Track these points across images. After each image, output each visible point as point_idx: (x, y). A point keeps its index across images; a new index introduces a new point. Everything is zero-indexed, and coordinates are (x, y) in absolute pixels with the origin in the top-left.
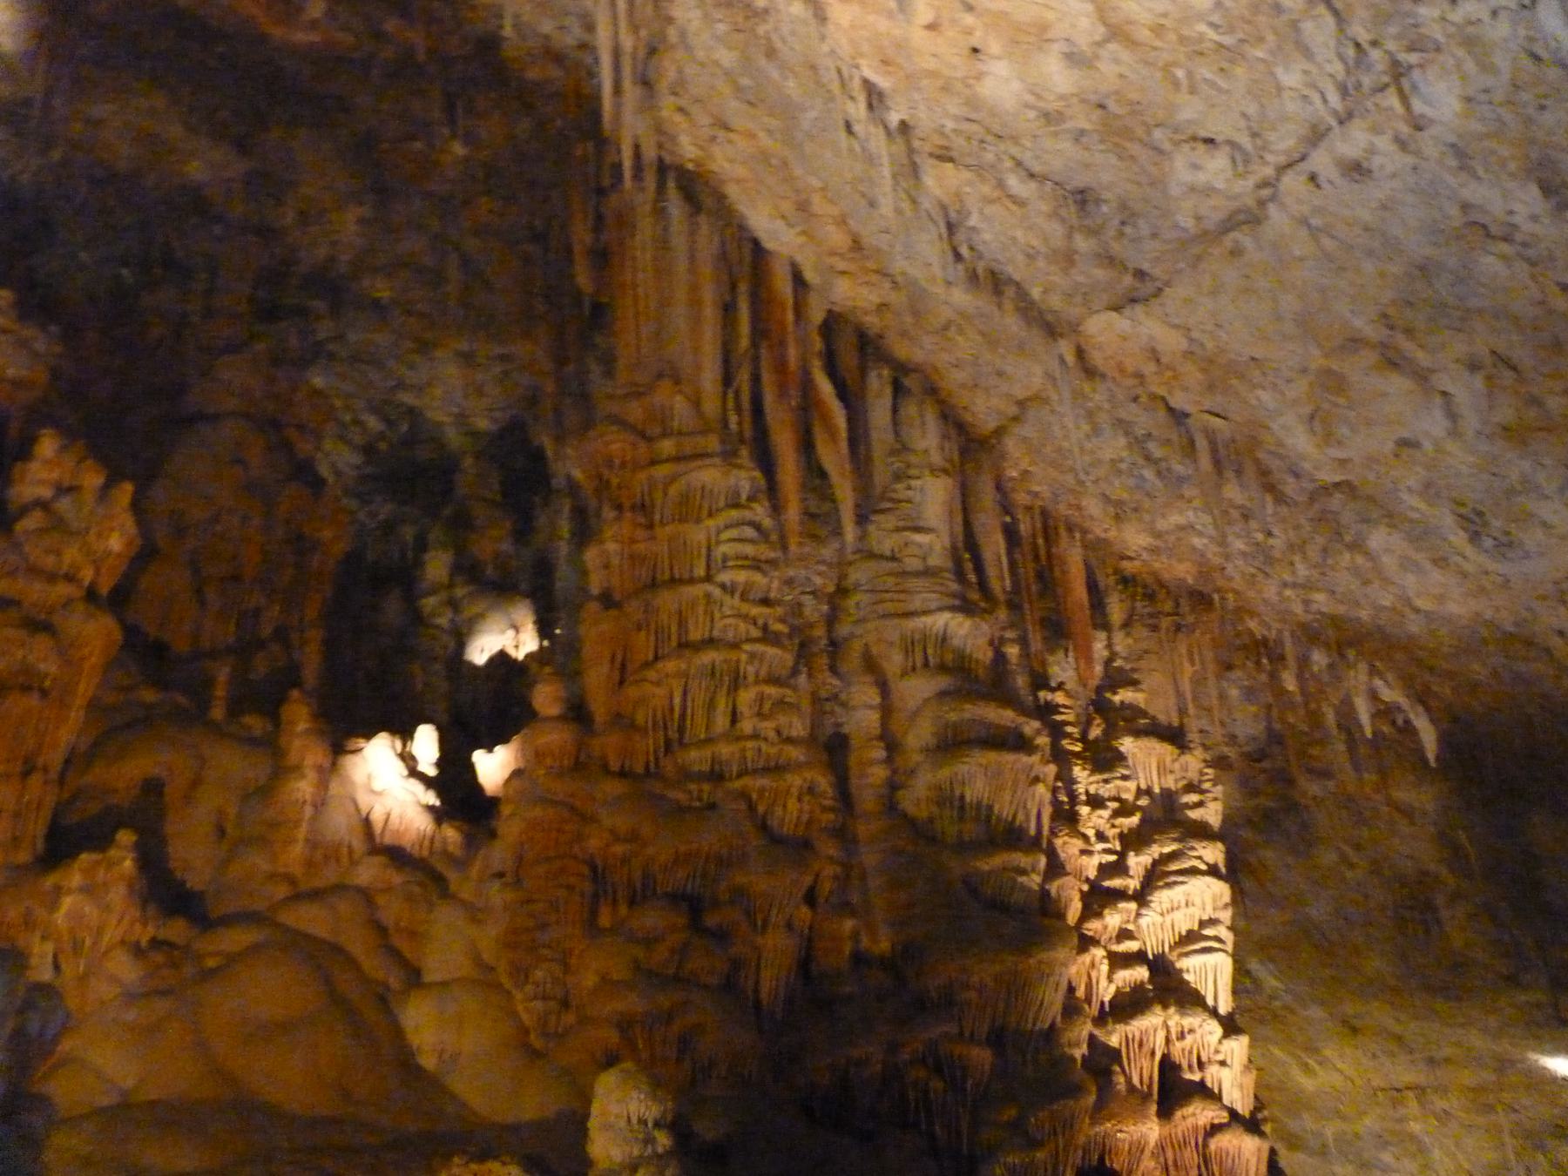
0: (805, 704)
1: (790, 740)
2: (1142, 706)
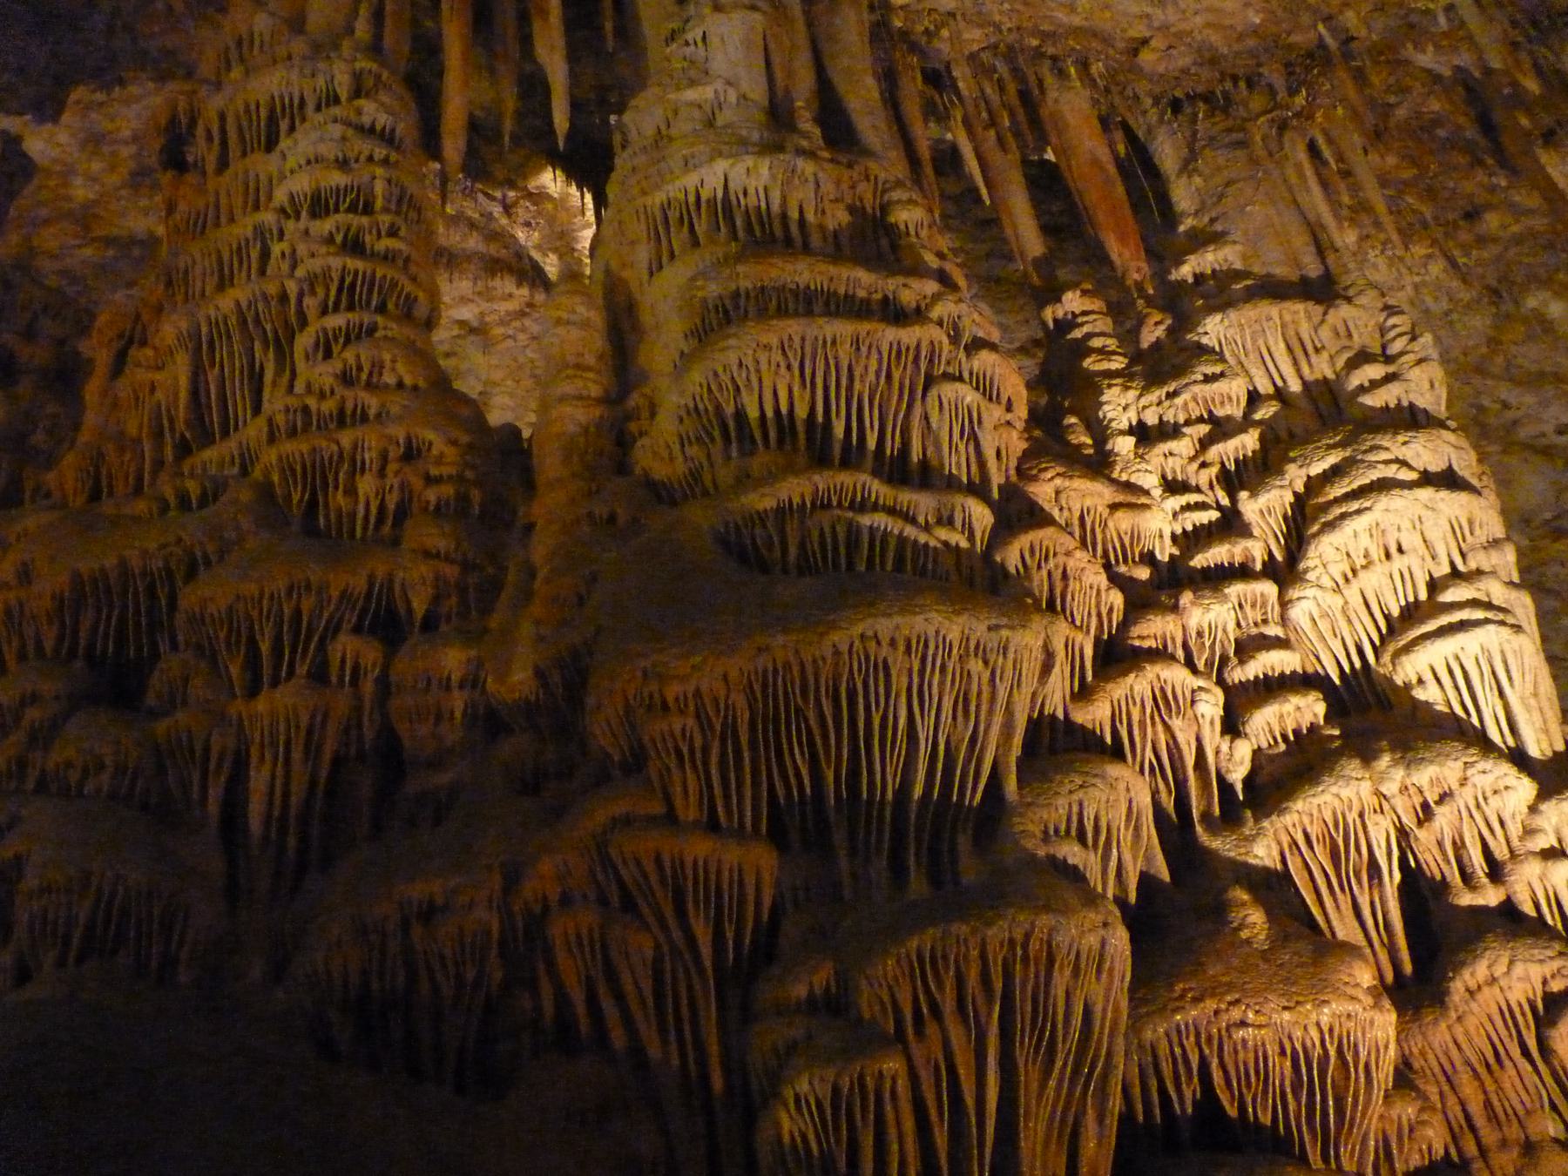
2: (1238, 265)
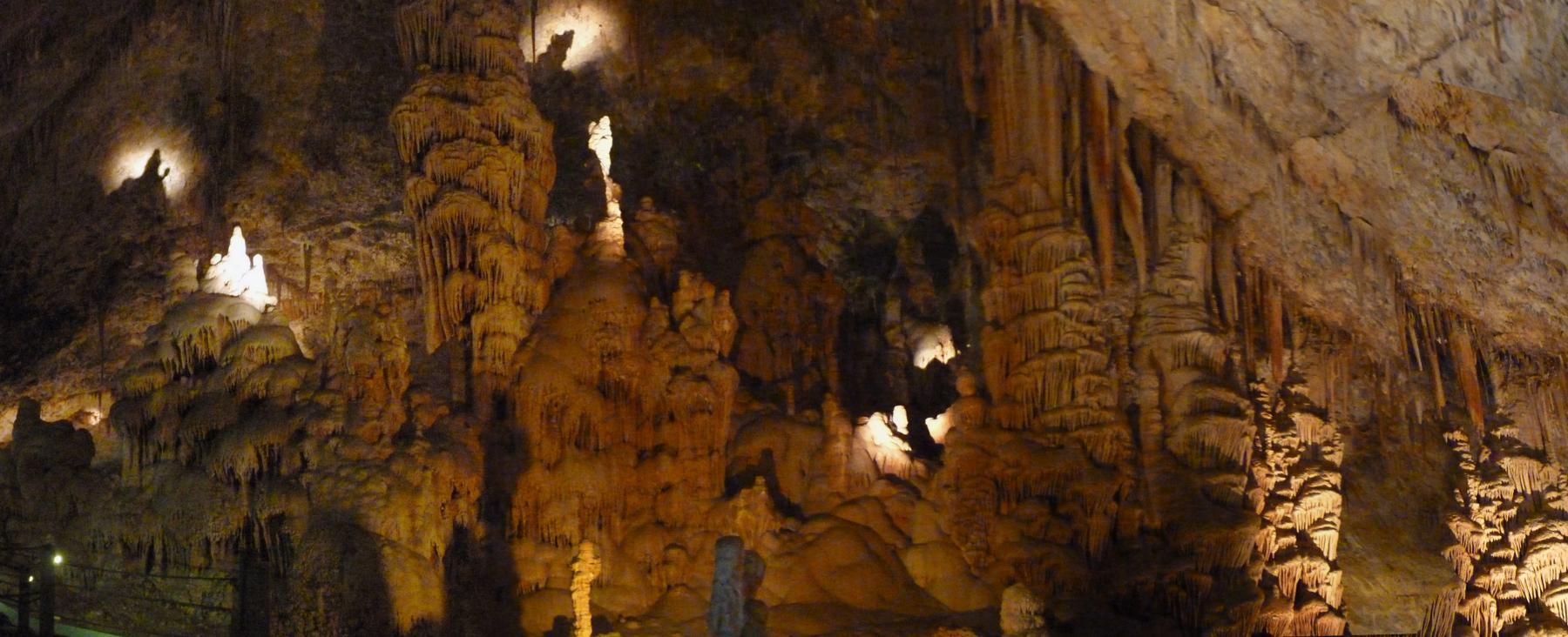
0: (1115, 387)
1: (1106, 408)
